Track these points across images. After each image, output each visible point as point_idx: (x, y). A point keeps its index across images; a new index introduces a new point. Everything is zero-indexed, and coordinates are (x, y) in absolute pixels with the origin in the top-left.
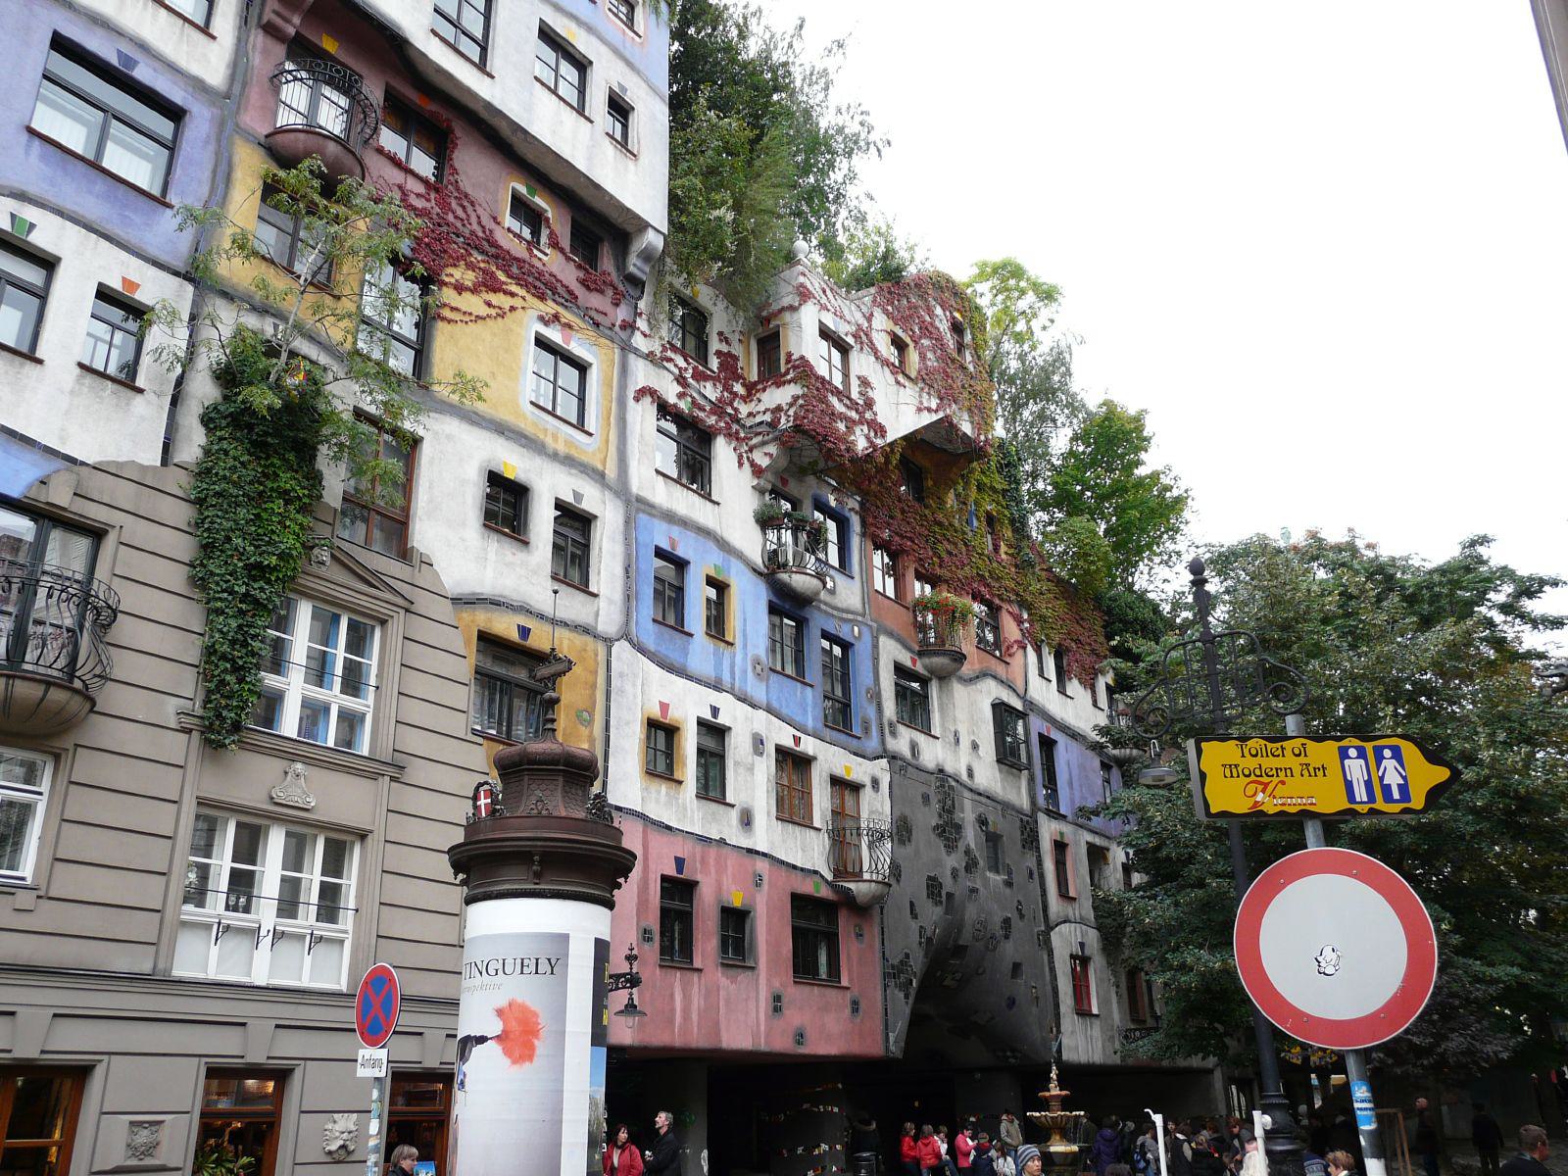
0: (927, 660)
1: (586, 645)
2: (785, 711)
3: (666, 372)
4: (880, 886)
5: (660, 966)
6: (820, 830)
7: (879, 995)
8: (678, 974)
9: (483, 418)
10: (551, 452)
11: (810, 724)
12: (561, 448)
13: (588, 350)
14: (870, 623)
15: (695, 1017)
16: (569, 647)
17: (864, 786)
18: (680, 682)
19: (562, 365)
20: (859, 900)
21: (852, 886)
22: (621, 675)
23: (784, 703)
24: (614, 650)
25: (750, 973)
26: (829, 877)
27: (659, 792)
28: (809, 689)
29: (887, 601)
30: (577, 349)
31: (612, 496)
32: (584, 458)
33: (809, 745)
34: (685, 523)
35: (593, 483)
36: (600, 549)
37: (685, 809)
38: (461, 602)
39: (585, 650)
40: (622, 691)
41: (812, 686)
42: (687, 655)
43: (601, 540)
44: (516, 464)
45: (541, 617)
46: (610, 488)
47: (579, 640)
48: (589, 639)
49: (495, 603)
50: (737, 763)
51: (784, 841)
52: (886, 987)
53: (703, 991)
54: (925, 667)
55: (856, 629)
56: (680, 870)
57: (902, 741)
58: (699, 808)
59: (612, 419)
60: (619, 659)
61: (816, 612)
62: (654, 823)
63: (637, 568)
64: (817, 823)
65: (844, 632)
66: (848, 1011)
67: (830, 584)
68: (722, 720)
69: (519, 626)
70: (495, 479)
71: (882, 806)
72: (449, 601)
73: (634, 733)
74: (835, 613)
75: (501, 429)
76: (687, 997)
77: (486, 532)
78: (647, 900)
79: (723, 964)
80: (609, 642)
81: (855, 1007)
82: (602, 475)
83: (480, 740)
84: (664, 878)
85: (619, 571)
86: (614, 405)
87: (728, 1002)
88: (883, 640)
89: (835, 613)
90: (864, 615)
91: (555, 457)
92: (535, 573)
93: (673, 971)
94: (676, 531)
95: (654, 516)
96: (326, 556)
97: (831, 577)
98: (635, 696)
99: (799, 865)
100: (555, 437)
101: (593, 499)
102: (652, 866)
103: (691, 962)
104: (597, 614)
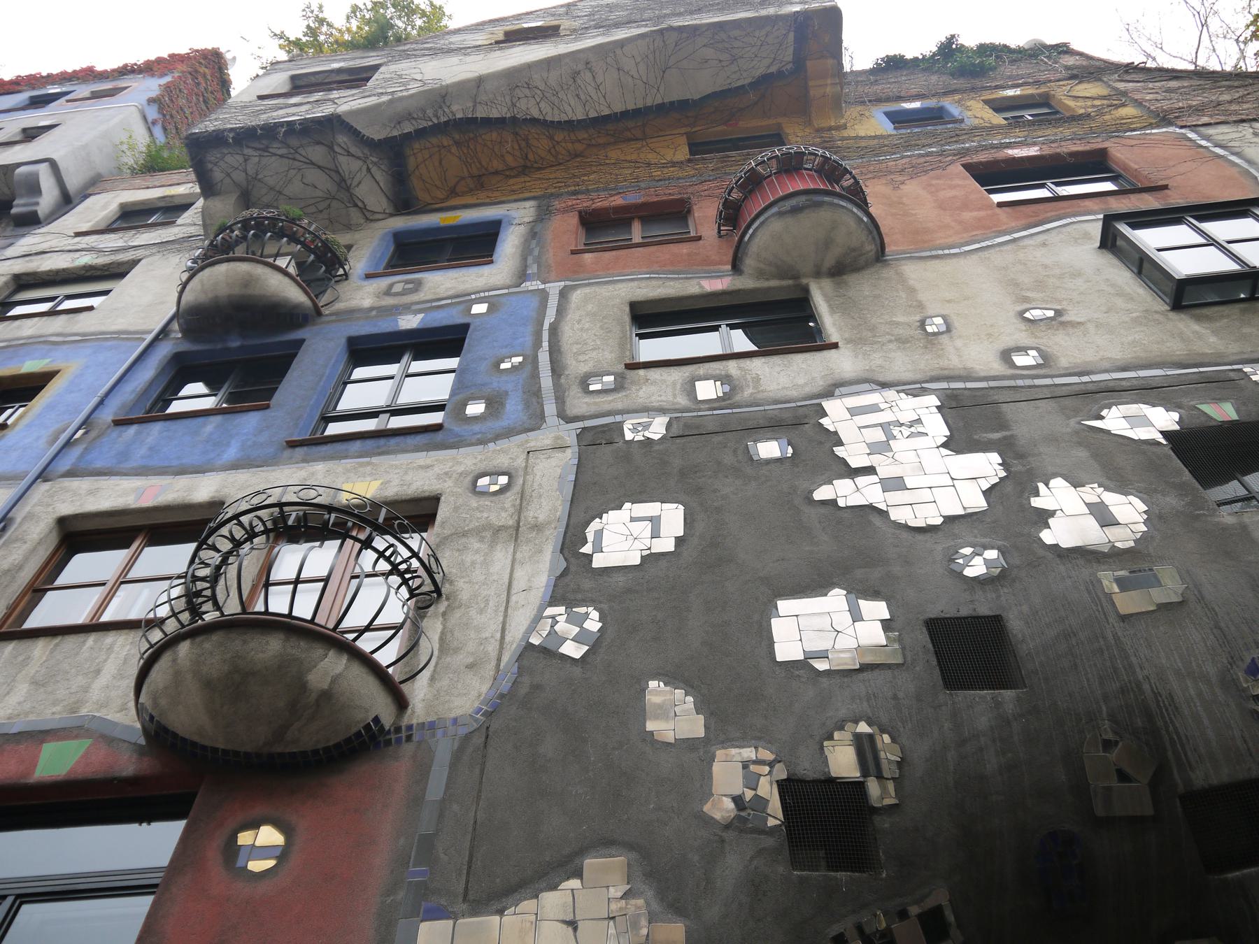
0: (749, 263)
54: (761, 274)
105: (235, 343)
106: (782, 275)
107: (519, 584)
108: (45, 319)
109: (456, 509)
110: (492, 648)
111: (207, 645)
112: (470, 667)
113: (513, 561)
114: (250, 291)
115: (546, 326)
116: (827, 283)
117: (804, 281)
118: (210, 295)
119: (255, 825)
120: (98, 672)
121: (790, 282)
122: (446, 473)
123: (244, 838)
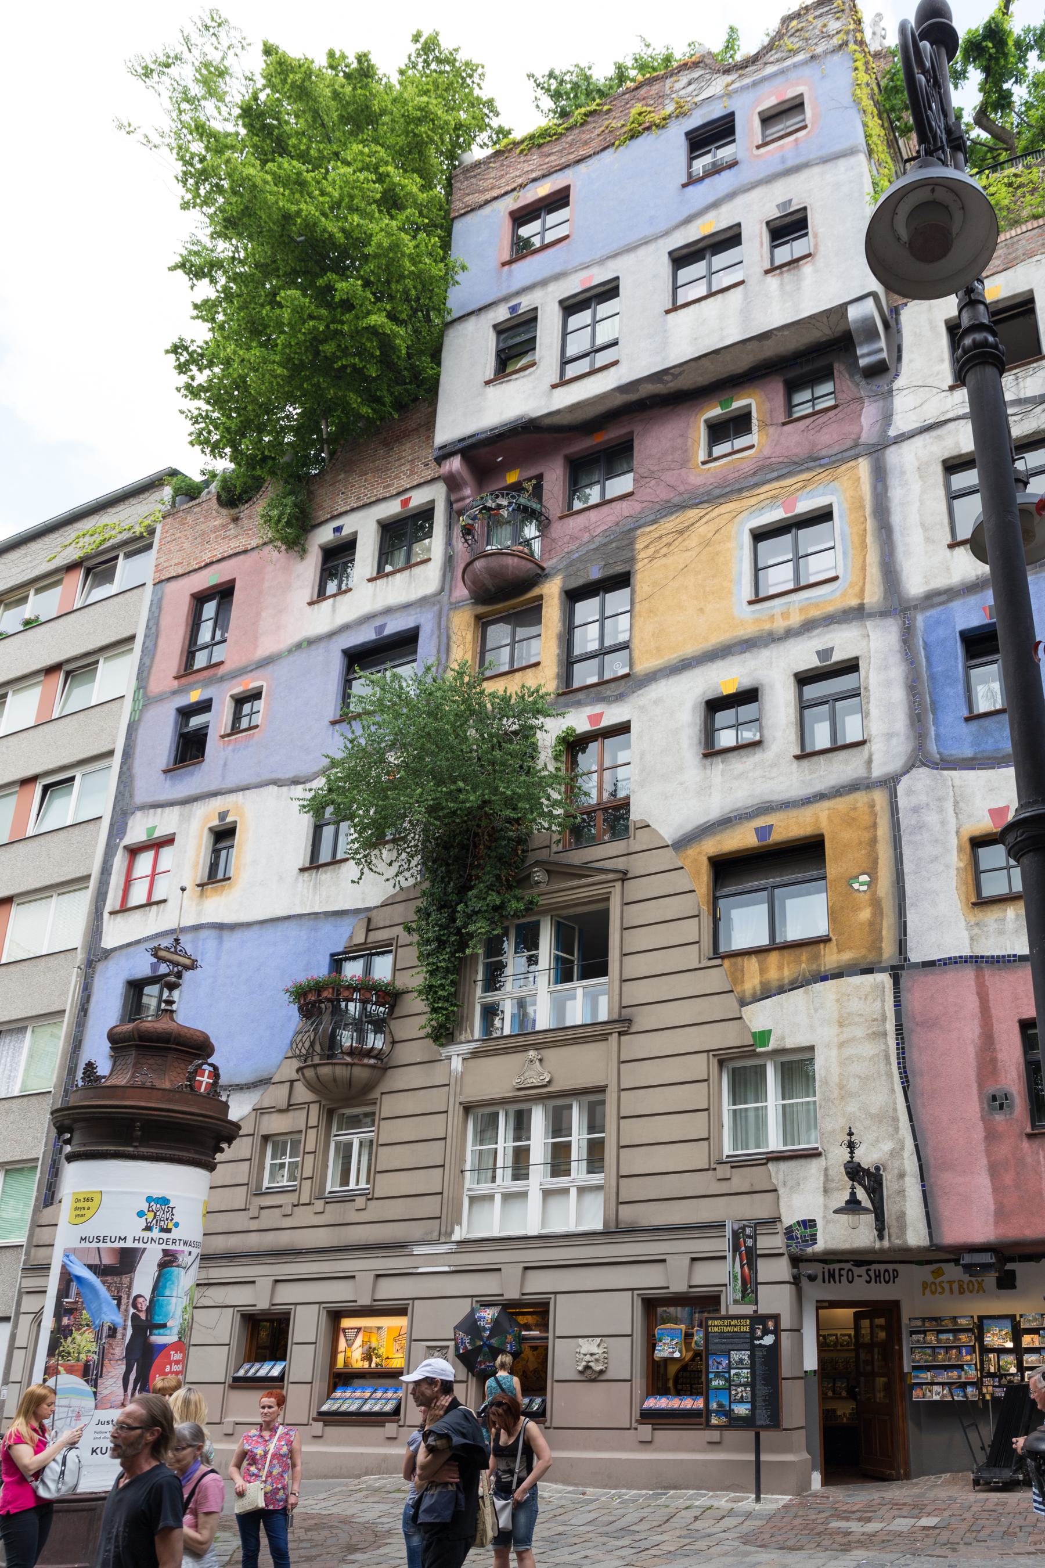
1: (857, 802)
3: (951, 426)
5: (1029, 1136)
10: (782, 631)
12: (795, 620)
13: (823, 494)
16: (829, 818)
19: (803, 533)
22: (916, 810)
24: (901, 789)
27: (1004, 920)
30: (804, 505)
31: (878, 621)
32: (830, 609)
35: (844, 626)
38: (682, 844)
39: (855, 809)
40: (921, 827)
43: (867, 677)
44: (728, 677)
45: (787, 805)
46: (872, 615)
47: (841, 804)
48: (860, 798)
49: (725, 823)
59: (869, 539)
60: (910, 792)
69: (756, 829)
70: (715, 705)
72: (670, 852)
73: (947, 866)
75: (685, 665)
77: (708, 762)
78: (994, 1061)
80: (890, 783)
83: (718, 962)
85: (898, 695)
86: (870, 524)
91: (789, 634)
92: (773, 765)
95: (950, 600)
96: (539, 876)
98: (943, 823)
100: (785, 615)
101: (843, 643)
102: (996, 1011)
104: (870, 761)
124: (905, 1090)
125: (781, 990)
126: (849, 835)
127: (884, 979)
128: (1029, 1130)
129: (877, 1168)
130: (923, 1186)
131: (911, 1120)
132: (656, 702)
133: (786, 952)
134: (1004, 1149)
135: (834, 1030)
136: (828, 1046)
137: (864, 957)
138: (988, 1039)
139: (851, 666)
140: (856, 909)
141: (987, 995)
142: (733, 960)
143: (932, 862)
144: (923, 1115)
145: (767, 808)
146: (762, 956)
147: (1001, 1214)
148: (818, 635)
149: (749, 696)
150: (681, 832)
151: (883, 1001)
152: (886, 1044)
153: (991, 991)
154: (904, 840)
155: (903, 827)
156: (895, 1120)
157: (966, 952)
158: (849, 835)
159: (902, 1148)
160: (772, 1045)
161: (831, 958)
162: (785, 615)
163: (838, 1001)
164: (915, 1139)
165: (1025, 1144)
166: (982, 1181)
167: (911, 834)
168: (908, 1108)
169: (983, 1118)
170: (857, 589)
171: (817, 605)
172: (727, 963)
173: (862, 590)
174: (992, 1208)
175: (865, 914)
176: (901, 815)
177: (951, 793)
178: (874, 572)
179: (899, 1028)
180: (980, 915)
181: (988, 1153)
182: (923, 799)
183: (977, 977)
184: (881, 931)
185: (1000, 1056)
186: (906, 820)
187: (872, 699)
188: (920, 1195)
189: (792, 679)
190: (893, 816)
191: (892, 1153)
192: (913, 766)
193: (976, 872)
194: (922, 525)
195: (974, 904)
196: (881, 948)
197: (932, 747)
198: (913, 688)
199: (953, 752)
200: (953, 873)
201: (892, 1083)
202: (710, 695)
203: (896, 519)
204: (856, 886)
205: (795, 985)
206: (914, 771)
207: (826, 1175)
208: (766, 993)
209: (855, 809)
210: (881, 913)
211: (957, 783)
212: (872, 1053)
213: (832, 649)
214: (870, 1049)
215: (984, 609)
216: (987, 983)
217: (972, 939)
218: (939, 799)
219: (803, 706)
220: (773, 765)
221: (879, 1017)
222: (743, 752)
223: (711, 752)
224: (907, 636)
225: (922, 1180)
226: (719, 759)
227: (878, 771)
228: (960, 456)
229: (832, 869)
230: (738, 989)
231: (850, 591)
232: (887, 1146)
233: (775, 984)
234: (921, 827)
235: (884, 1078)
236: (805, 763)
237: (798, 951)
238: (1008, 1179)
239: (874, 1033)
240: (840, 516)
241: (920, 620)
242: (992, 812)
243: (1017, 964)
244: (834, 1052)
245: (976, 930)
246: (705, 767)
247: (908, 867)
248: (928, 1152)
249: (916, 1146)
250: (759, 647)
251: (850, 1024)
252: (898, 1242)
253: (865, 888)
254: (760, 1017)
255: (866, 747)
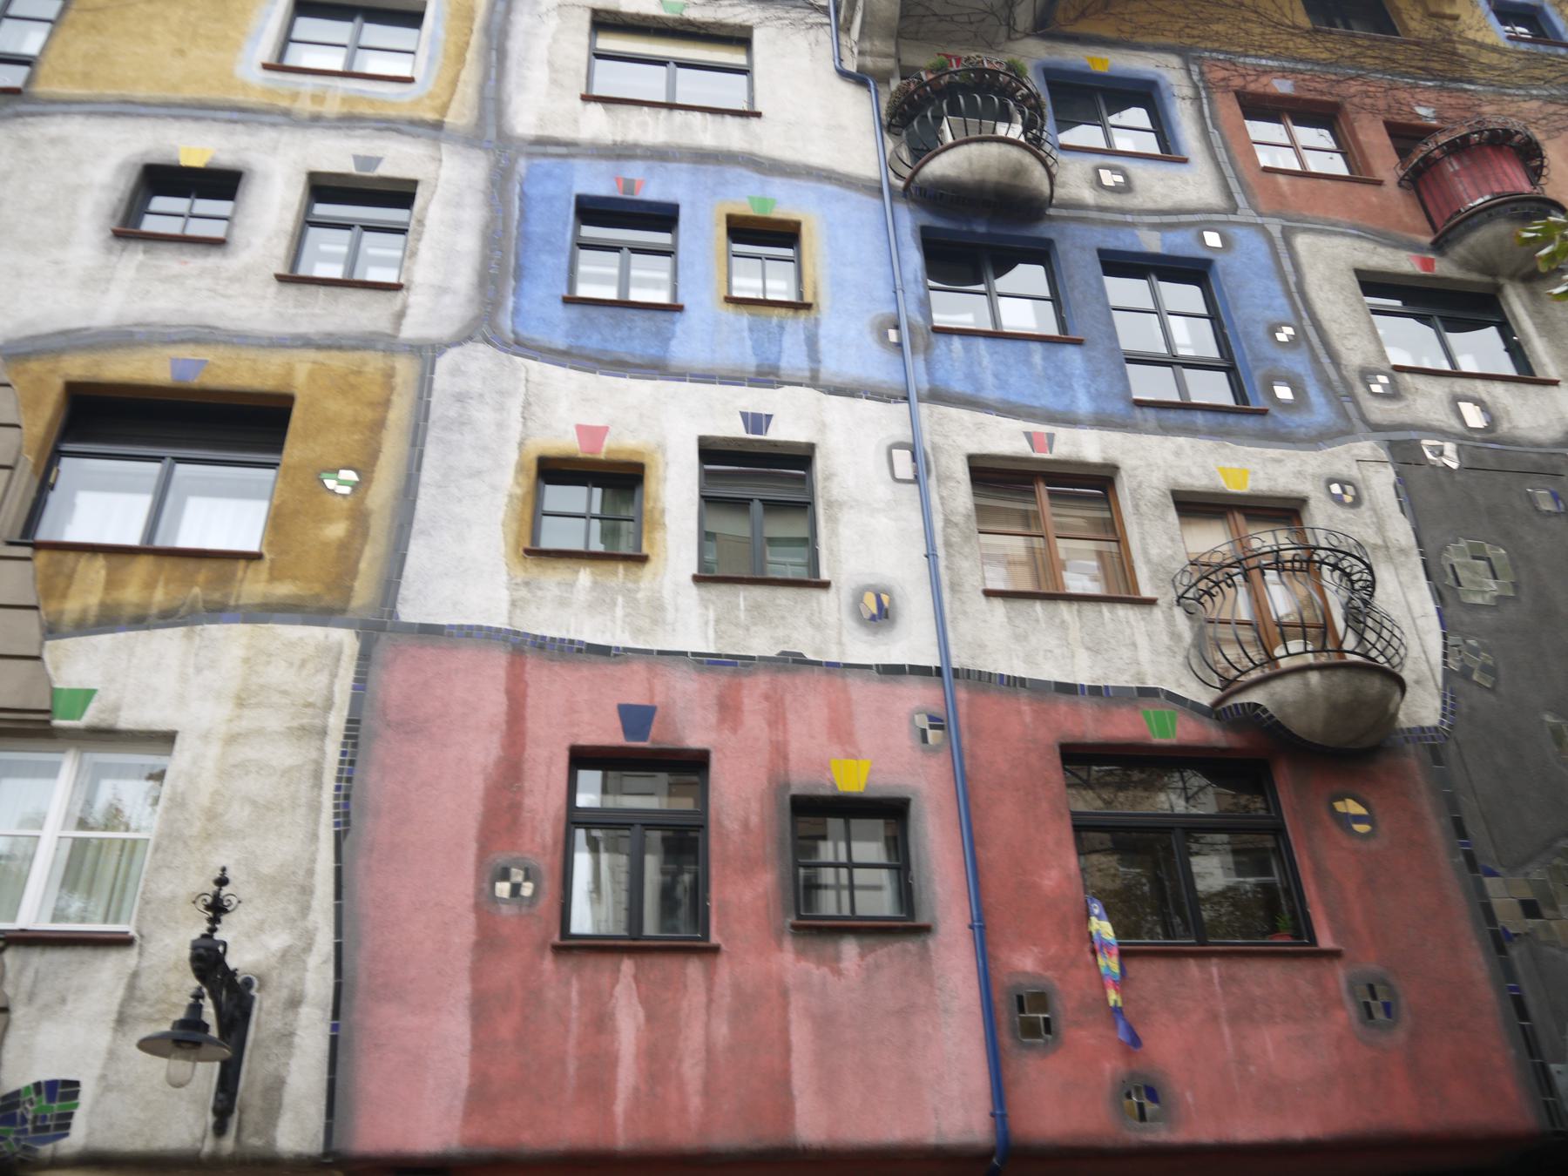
0: (1460, 250)
2: (991, 394)
4: (1339, 677)
6: (1151, 602)
7: (1476, 963)
8: (627, 966)
9: (145, 104)
10: (306, 115)
11: (1084, 405)
12: (332, 108)
14: (1259, 220)
15: (692, 1070)
16: (312, 376)
17: (1303, 501)
18: (641, 389)
20: (1298, 725)
21: (1255, 696)
22: (461, 398)
23: (989, 380)
24: (443, 363)
25: (911, 945)
26: (1205, 698)
27: (572, 585)
28: (1072, 354)
29: (1302, 183)
32: (392, 113)
33: (1085, 445)
34: (660, 155)
36: (421, 222)
37: (657, 606)
39: (359, 373)
40: (463, 423)
41: (1078, 342)
42: (665, 339)
43: (425, 209)
49: (122, 338)
50: (830, 504)
51: (1020, 638)
52: (1499, 941)
53: (725, 998)
54: (1464, 264)
55: (1212, 239)
56: (628, 731)
57: (1427, 403)
58: (704, 604)
59: (471, 55)
60: (456, 371)
61: (1072, 228)
62: (542, 645)
63: (524, 237)
64: (1146, 591)
65: (1176, 243)
66: (1347, 1015)
67: (1108, 178)
68: (779, 432)
71: (1380, 528)
73: (494, 488)
74: (1137, 219)
76: (661, 1020)
78: (516, 808)
79: (797, 929)
81: (1376, 1003)
82: (438, 126)
84: (582, 758)
85: (468, 243)
86: (476, 40)
87: (825, 1023)
88: (1302, 242)
89: (1137, 219)
90: (1234, 209)
91: (316, 120)
92: (233, 279)
93: (606, 962)
94: (634, 170)
97: (1114, 169)
98: (501, 426)
99: (1083, 677)
103: (706, 937)
104: (401, 315)
105: (981, 229)
106: (1483, 270)
107: (1417, 611)
108: (708, 116)
109: (1330, 518)
110: (1425, 667)
111: (1335, 679)
112: (1417, 682)
113: (1400, 583)
114: (1017, 182)
115: (1293, 288)
116: (1521, 288)
117: (1501, 281)
118: (977, 177)
119: (1342, 798)
120: (1134, 645)
121: (1486, 279)
122: (1299, 474)
123: (1340, 806)
124: (339, 839)
125: (140, 621)
126: (335, 406)
127: (345, 639)
128: (556, 939)
129: (248, 983)
130: (335, 1027)
131: (338, 894)
132: (53, 141)
133: (168, 563)
134: (507, 970)
135: (226, 710)
136: (205, 737)
137: (317, 596)
138: (510, 772)
139: (400, 194)
140: (323, 517)
141: (524, 695)
142: (57, 555)
143: (471, 476)
144: (363, 888)
145: (203, 335)
146: (117, 560)
147: (480, 1097)
148: (363, 137)
149: (221, 183)
150: (29, 332)
151: (334, 675)
152: (322, 750)
153: (531, 692)
154: (433, 434)
155: (433, 416)
156: (307, 891)
157: (500, 621)
158: (335, 406)
159: (308, 948)
160: (90, 717)
161: (253, 586)
162: (317, 98)
163: (246, 660)
164: (338, 932)
165: (548, 963)
166: (456, 1028)
167: (445, 428)
168: (338, 872)
169: (477, 908)
170: (438, 102)
171: (371, 102)
172: (42, 557)
173: (444, 108)
174: (465, 1081)
175: (336, 530)
176: (434, 400)
177: (522, 389)
178: (467, 90)
179: (353, 724)
180: (534, 570)
181: (476, 974)
182: (476, 385)
183: (512, 664)
184: (357, 562)
185: (528, 802)
186: (440, 408)
187: (426, 237)
188: (324, 1045)
189: (303, 178)
190: (421, 398)
191: (285, 956)
192: (470, 338)
193: (537, 513)
194: (551, 64)
195: (528, 552)
196: (351, 589)
197: (506, 323)
198: (493, 238)
199: (537, 337)
200: (502, 500)
201: (316, 822)
202: (156, 159)
203: (515, 46)
204: (330, 484)
205: (169, 618)
206: (469, 346)
207: (131, 987)
208: (108, 620)
209: (359, 373)
210: (365, 535)
211: (534, 377)
212: (289, 762)
213: (379, 160)
214: (287, 755)
215: (617, 180)
216: (527, 677)
217: (513, 604)
218: (502, 393)
219: (309, 221)
220: (233, 279)
221: (319, 702)
222: (186, 248)
223: (128, 229)
224: (499, 181)
225: (336, 1013)
226: (141, 246)
227: (409, 331)
228: (617, 14)
229: (294, 449)
230: (52, 606)
231: (428, 102)
232: (278, 941)
233: (129, 611)
234: (463, 423)
235: (303, 811)
236: (292, 290)
237: (191, 564)
238: (505, 1027)
239: (303, 728)
240: (436, 18)
241: (522, 165)
242: (581, 429)
243: (581, 656)
244: (214, 751)
245: (523, 592)
246: (109, 251)
247: (428, 475)
248: (358, 962)
249: (338, 948)
250: (262, 123)
251: (259, 705)
252: (254, 1142)
253: (346, 490)
254: (80, 664)
255: (400, 295)
